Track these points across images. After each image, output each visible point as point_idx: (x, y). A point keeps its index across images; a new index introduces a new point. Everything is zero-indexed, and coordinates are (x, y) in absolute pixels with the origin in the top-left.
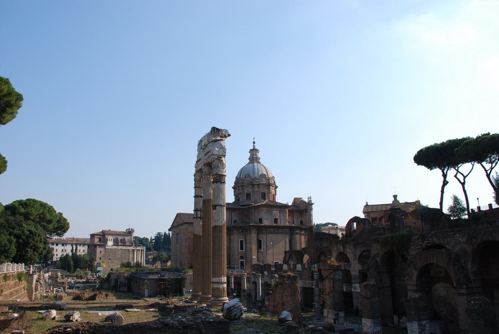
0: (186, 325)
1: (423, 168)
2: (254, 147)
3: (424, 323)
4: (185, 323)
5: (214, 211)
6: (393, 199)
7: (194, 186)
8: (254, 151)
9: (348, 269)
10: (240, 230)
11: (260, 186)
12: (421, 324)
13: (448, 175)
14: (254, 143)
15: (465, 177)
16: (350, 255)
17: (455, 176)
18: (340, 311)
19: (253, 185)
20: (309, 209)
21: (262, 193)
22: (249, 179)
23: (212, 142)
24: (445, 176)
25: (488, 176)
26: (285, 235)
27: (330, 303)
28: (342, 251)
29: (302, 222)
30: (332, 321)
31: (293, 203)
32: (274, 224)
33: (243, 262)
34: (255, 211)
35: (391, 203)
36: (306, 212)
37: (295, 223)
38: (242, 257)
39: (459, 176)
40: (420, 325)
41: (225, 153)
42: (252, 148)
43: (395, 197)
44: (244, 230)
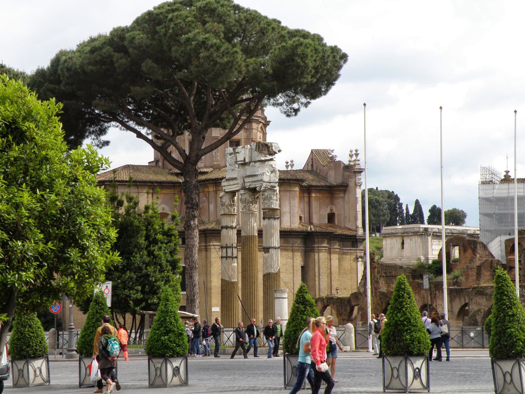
20: (351, 184)
23: (259, 161)
29: (331, 217)
31: (307, 164)
36: (345, 191)
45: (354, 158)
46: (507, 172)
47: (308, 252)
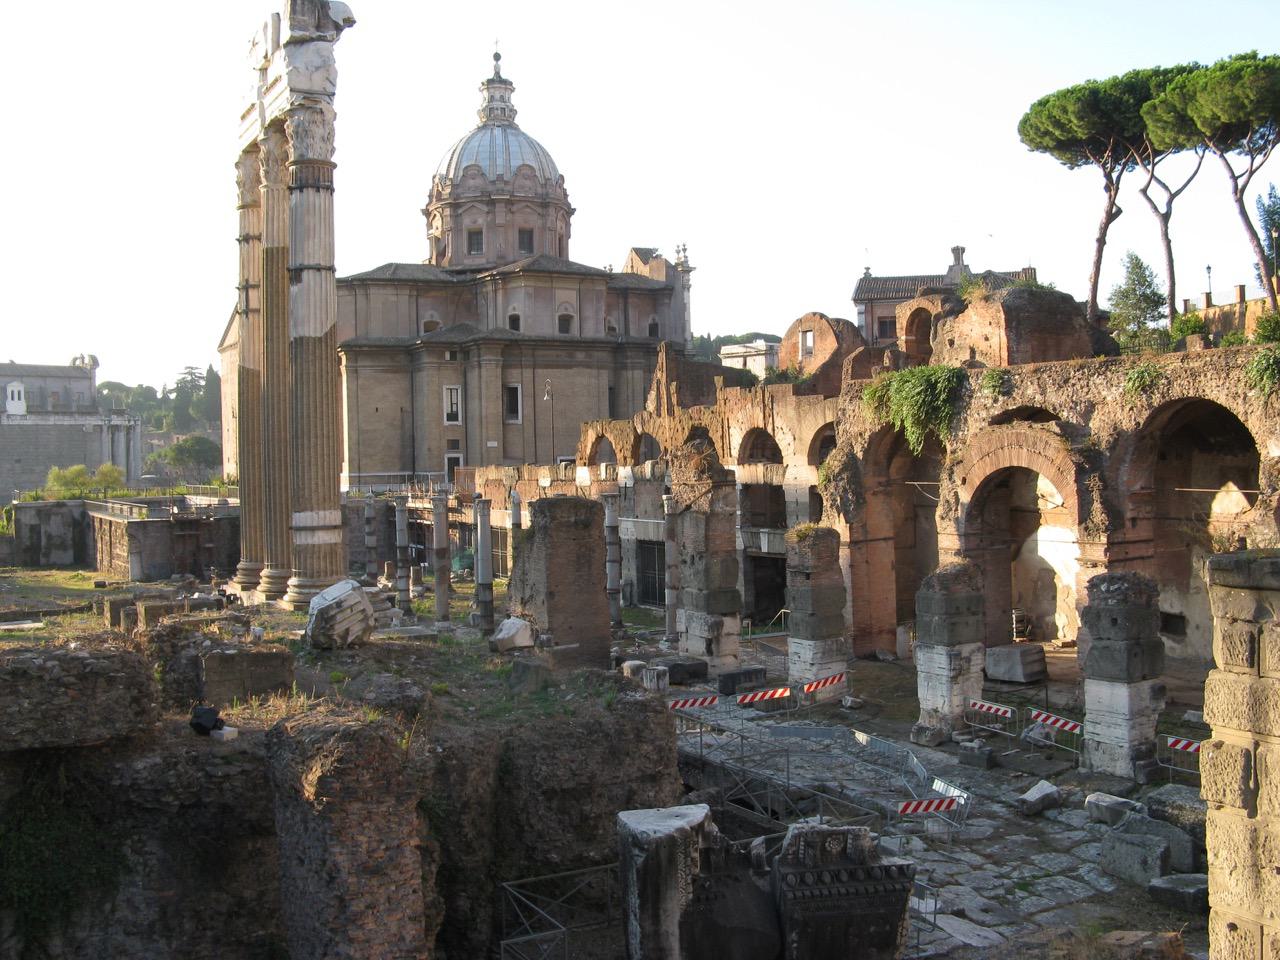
0: (88, 670)
1: (1049, 162)
2: (497, 73)
3: (966, 650)
4: (86, 666)
5: (294, 289)
6: (951, 260)
7: (237, 203)
8: (498, 85)
9: (775, 482)
10: (448, 356)
11: (514, 208)
12: (958, 655)
13: (1121, 185)
14: (497, 57)
15: (1173, 197)
16: (783, 440)
17: (1144, 191)
18: (725, 615)
19: (492, 203)
20: (678, 287)
21: (522, 232)
22: (479, 182)
24: (1112, 187)
25: (1239, 193)
26: (594, 372)
27: (695, 591)
28: (761, 425)
30: (701, 647)
32: (564, 336)
33: (458, 459)
34: (495, 291)
35: (943, 271)
37: (633, 333)
38: (454, 445)
39: (1155, 191)
40: (953, 657)
41: (334, 85)
42: (491, 75)
43: (958, 252)
44: (459, 356)
45: (682, 254)
46: (868, 269)
47: (618, 369)
